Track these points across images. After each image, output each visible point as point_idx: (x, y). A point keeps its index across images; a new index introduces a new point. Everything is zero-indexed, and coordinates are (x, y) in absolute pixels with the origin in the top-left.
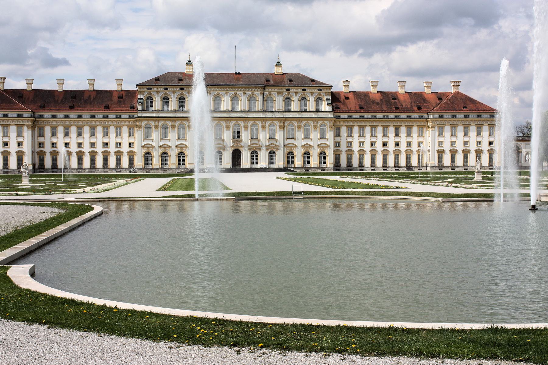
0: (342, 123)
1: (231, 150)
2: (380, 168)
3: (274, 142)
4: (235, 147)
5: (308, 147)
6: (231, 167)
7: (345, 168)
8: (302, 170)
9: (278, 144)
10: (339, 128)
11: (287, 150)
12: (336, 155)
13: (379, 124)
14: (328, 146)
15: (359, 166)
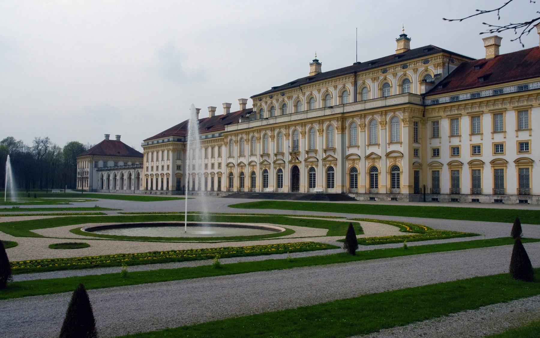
0: (442, 114)
1: (291, 166)
2: (511, 198)
3: (332, 153)
4: (294, 163)
5: (374, 159)
6: (290, 192)
7: (446, 197)
8: (366, 198)
9: (336, 156)
10: (438, 122)
11: (348, 165)
12: (433, 171)
13: (508, 106)
14: (402, 156)
15: (473, 193)
